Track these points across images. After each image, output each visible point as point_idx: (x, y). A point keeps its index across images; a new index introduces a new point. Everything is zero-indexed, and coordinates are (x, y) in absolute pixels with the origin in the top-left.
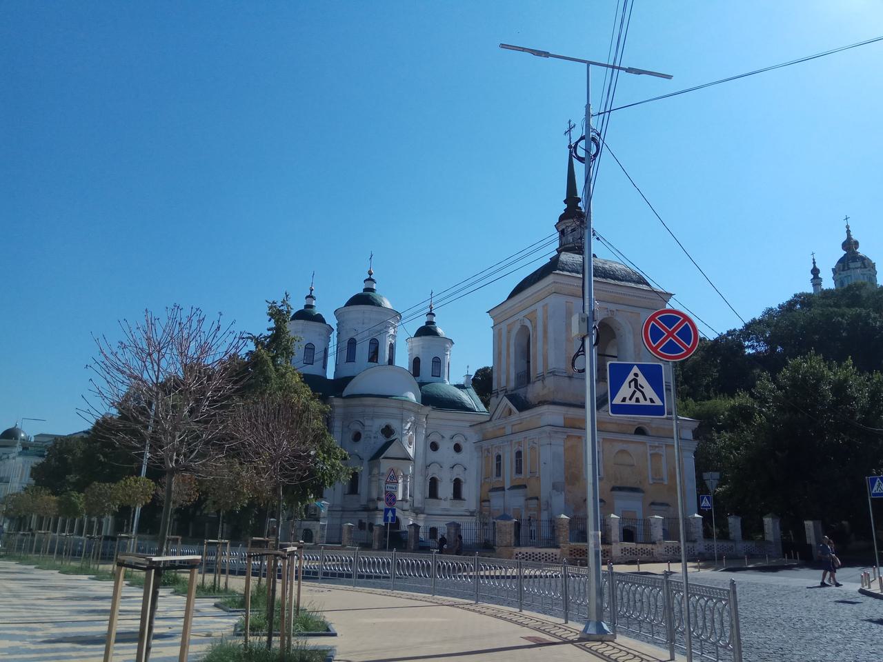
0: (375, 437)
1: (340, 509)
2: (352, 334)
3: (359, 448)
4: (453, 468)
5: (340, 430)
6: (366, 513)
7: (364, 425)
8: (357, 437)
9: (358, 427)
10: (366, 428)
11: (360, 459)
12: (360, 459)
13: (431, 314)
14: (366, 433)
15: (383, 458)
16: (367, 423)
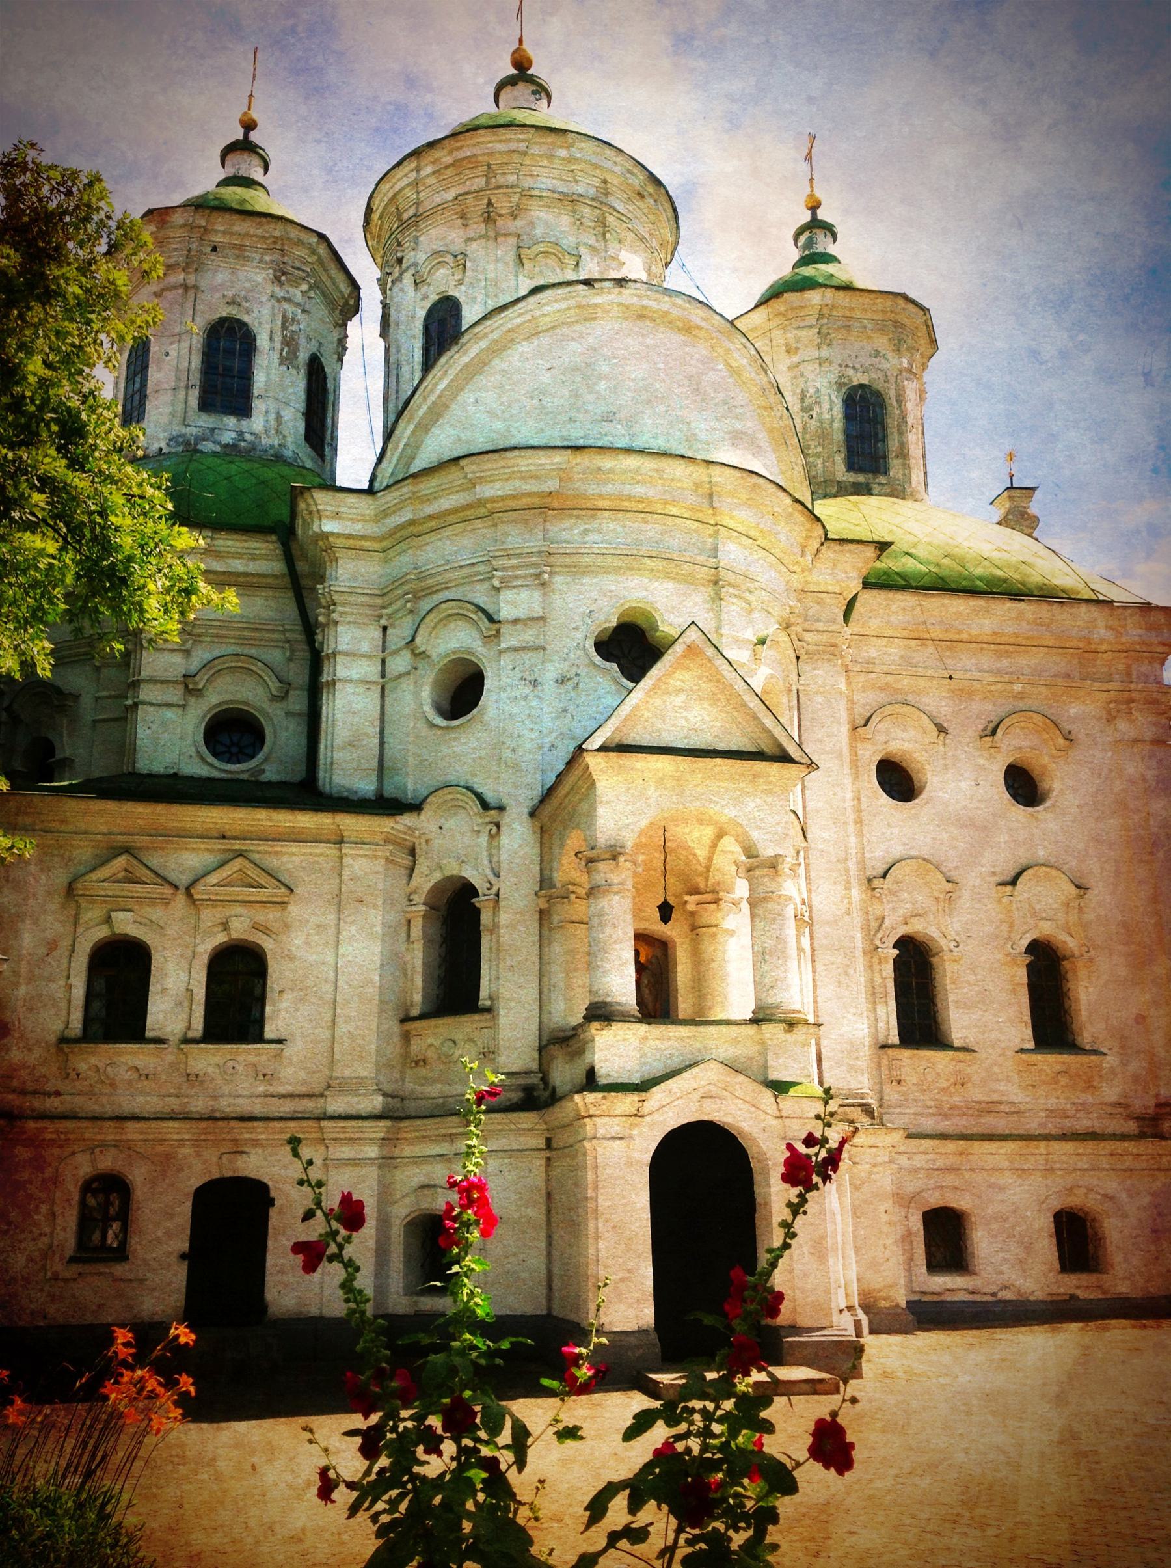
0: (562, 681)
1: (377, 1103)
2: (443, 282)
3: (466, 750)
4: (1013, 882)
5: (371, 670)
6: (527, 1119)
7: (491, 619)
8: (463, 693)
9: (455, 640)
10: (510, 639)
11: (485, 806)
12: (485, 806)
13: (816, 225)
14: (506, 660)
15: (603, 749)
16: (514, 603)
